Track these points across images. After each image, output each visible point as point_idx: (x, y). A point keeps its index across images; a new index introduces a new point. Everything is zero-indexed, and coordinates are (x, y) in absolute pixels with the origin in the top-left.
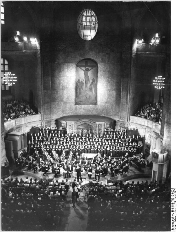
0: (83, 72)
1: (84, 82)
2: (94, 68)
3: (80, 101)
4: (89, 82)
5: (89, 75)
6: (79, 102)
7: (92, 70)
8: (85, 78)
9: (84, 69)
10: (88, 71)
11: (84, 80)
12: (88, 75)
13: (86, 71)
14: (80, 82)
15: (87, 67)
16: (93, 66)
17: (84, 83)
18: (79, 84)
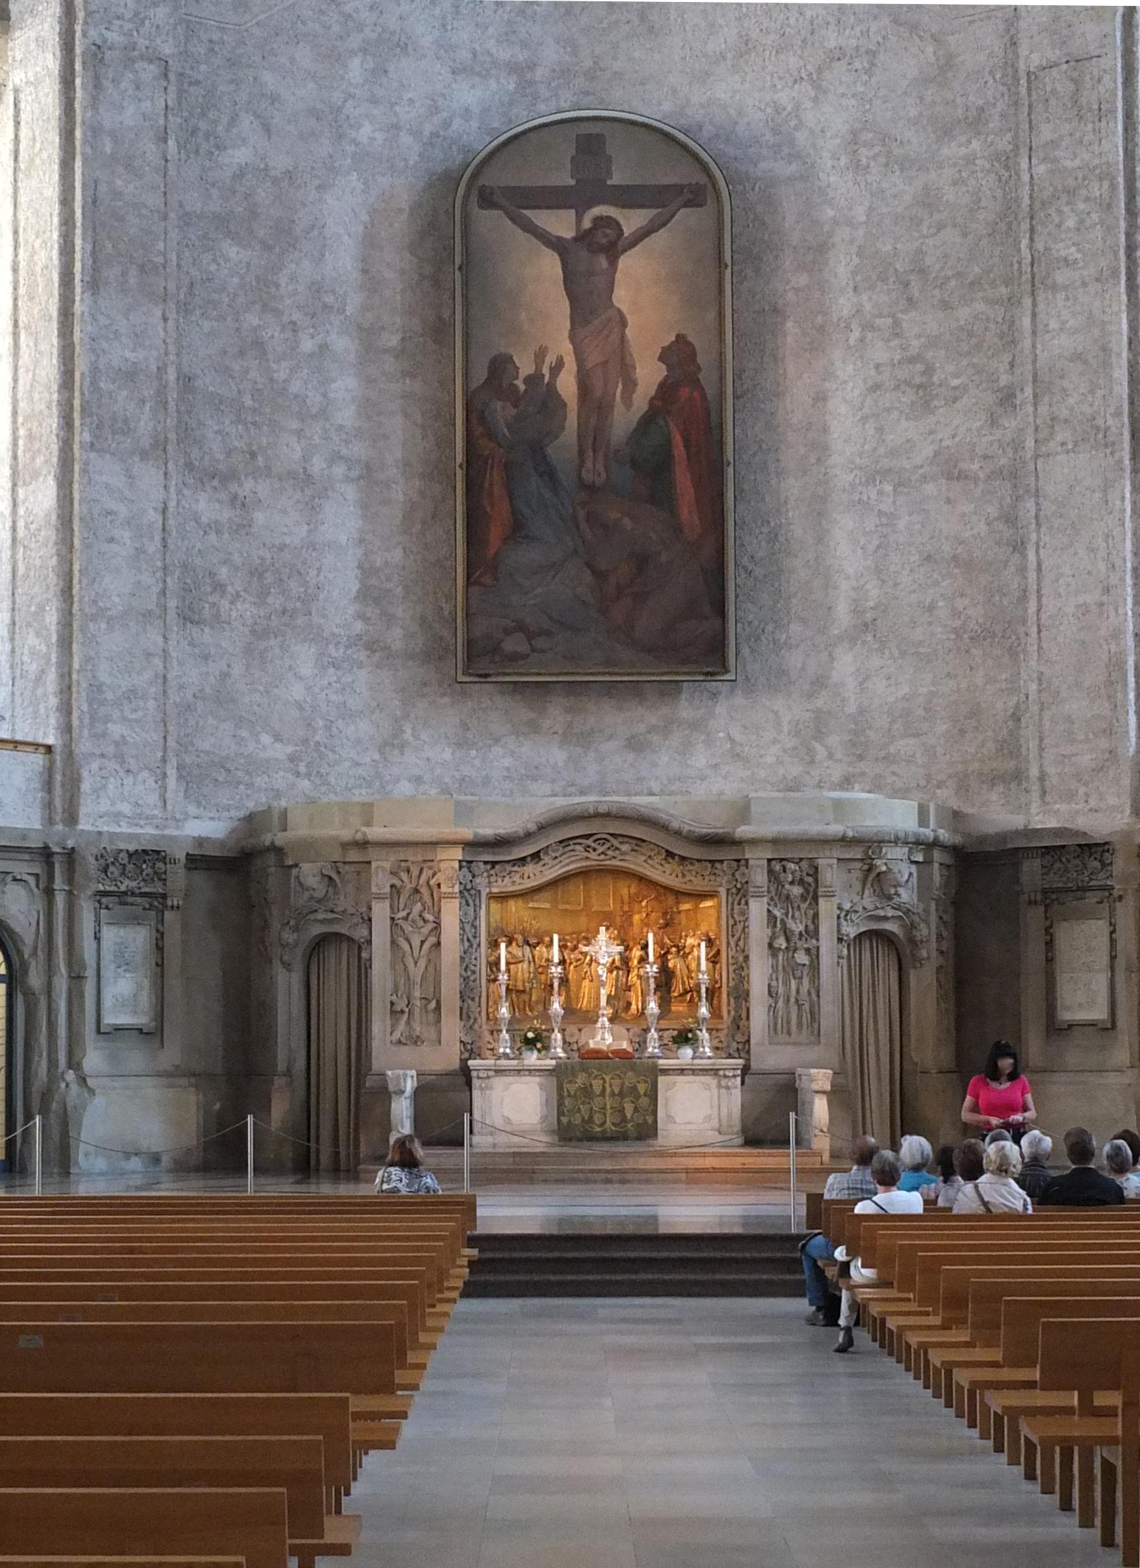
0: (551, 265)
1: (567, 385)
2: (683, 211)
3: (521, 627)
4: (631, 385)
5: (621, 297)
6: (507, 632)
7: (659, 239)
8: (572, 338)
9: (568, 233)
10: (613, 263)
11: (559, 365)
12: (612, 305)
13: (584, 254)
14: (522, 387)
15: (598, 211)
16: (678, 189)
17: (565, 405)
18: (501, 412)
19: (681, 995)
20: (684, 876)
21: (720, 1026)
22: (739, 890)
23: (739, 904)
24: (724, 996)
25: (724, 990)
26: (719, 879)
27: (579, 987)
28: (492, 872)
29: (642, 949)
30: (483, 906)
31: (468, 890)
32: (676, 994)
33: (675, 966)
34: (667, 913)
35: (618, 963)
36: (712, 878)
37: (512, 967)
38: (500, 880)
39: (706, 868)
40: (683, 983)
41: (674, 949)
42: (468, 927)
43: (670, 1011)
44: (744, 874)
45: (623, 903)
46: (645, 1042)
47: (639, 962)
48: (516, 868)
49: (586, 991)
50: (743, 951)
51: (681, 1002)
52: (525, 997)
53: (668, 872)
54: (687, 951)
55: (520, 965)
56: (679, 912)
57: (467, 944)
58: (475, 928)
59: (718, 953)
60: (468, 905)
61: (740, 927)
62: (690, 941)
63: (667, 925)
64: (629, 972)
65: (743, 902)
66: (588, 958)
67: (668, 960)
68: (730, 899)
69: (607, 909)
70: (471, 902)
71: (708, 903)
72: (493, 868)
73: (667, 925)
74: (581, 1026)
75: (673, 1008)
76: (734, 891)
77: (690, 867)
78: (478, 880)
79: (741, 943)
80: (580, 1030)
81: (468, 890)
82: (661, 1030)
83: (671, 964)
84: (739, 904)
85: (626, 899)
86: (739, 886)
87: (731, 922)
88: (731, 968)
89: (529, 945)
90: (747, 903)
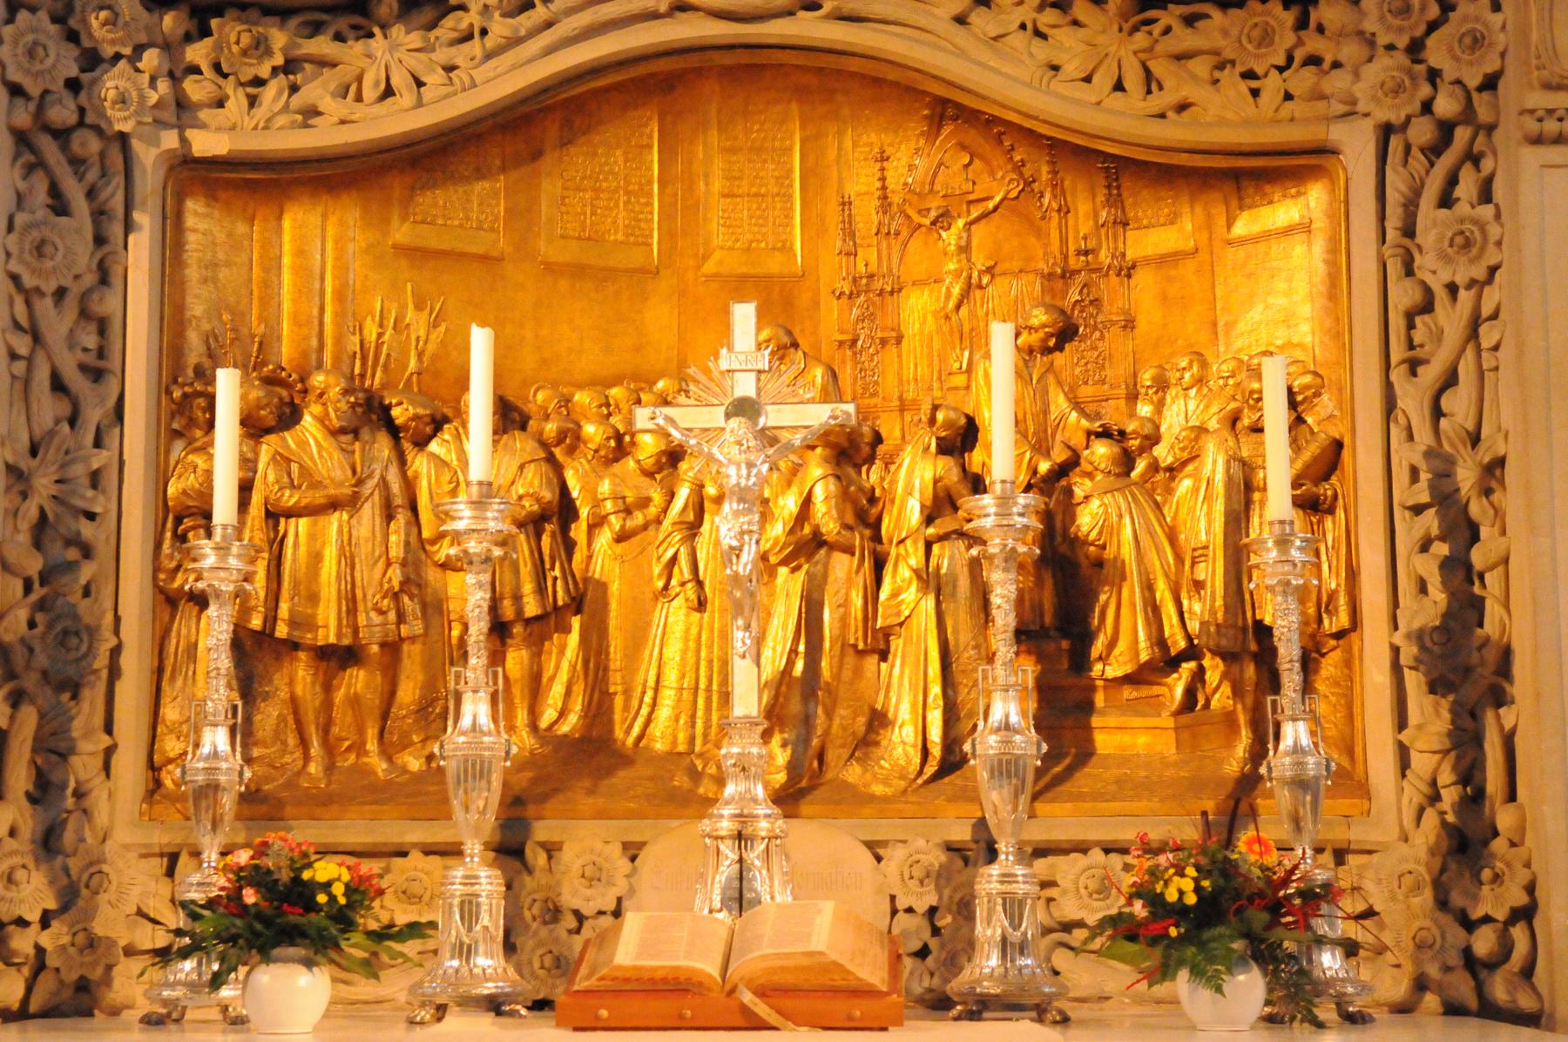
19: (1138, 677)
20: (1150, 81)
21: (1358, 834)
22: (1446, 130)
23: (1446, 201)
24: (1376, 677)
25: (1375, 641)
26: (1338, 82)
27: (638, 638)
28: (198, 53)
29: (945, 448)
30: (144, 219)
31: (62, 135)
32: (1111, 672)
33: (1109, 528)
34: (1067, 275)
35: (826, 517)
36: (1303, 79)
37: (300, 527)
38: (236, 100)
39: (1266, 38)
40: (1154, 611)
41: (1102, 451)
42: (57, 323)
43: (1086, 753)
44: (1477, 42)
45: (849, 232)
46: (965, 909)
47: (929, 520)
48: (322, 45)
49: (673, 651)
50: (1475, 439)
51: (1131, 708)
52: (357, 680)
53: (1072, 68)
54: (1164, 453)
55: (335, 521)
56: (1127, 271)
57: (48, 408)
58: (102, 327)
59: (1332, 458)
60: (59, 206)
61: (1450, 319)
62: (1179, 414)
63: (1065, 334)
64: (879, 565)
65: (1467, 188)
66: (683, 493)
67: (1069, 506)
68: (1396, 185)
69: (774, 265)
70: (75, 192)
71: (1282, 212)
72: (205, 32)
73: (1065, 334)
74: (636, 830)
75: (1100, 739)
76: (1422, 132)
77: (1185, 39)
78: (112, 83)
79: (1458, 404)
80: (633, 851)
81: (62, 135)
82: (1041, 852)
83: (1087, 520)
84: (1446, 200)
85: (867, 214)
86: (1446, 105)
87: (1403, 295)
88: (1409, 531)
89: (394, 431)
90: (1486, 195)
